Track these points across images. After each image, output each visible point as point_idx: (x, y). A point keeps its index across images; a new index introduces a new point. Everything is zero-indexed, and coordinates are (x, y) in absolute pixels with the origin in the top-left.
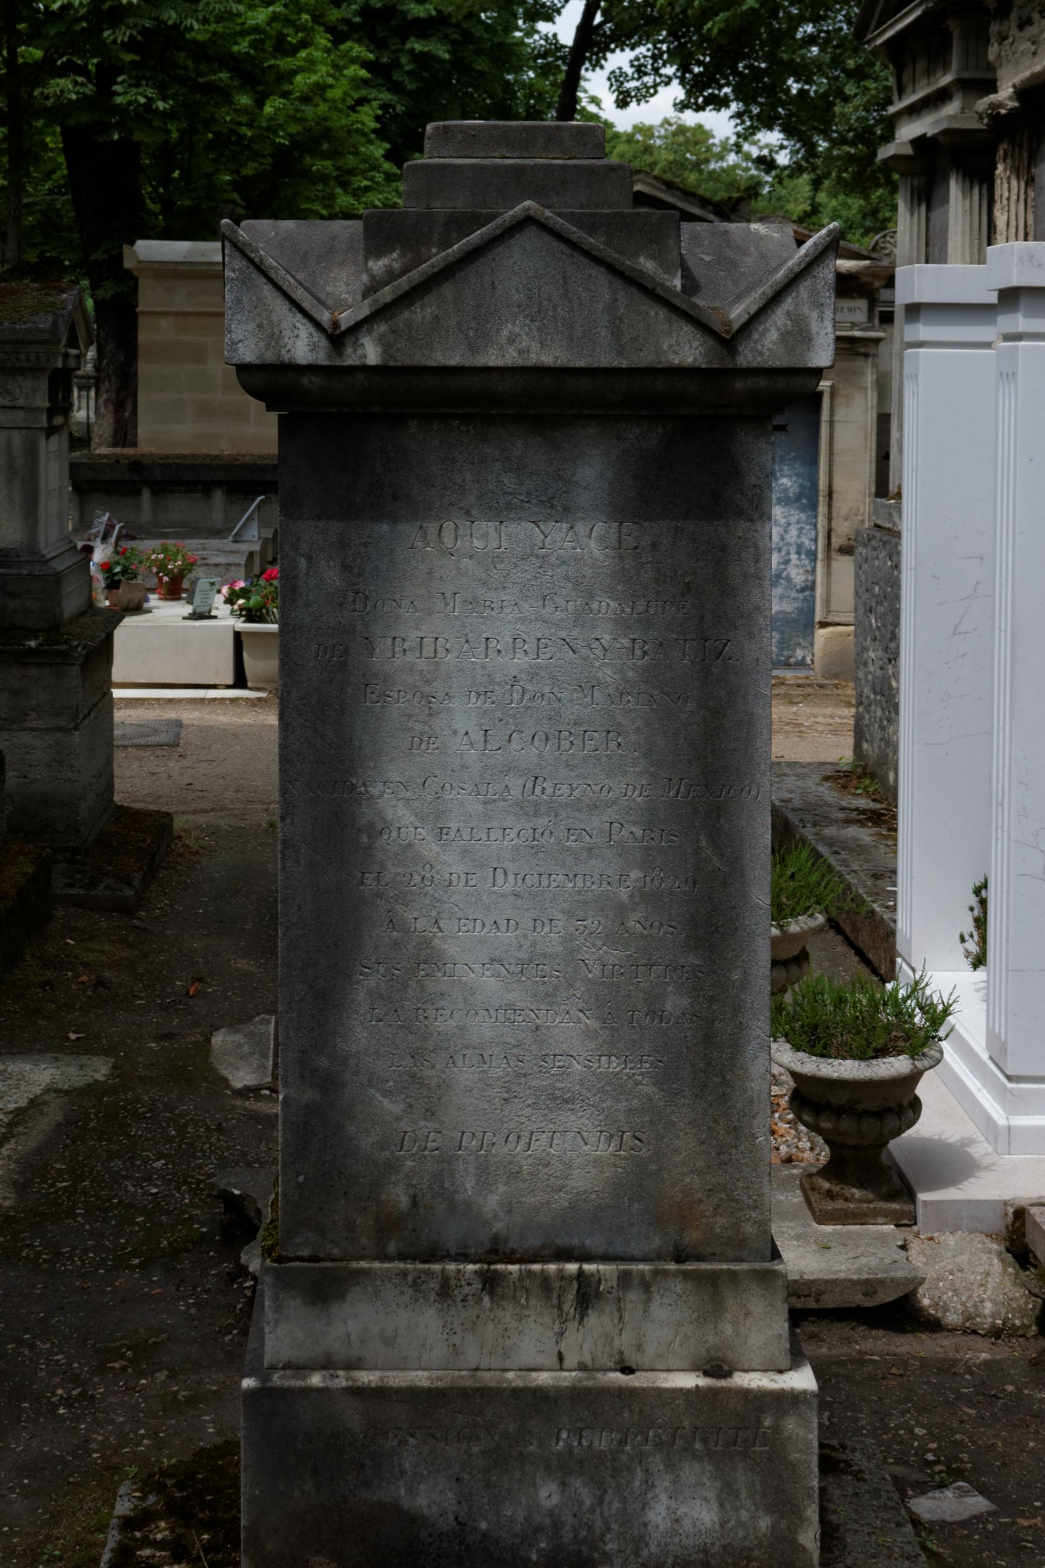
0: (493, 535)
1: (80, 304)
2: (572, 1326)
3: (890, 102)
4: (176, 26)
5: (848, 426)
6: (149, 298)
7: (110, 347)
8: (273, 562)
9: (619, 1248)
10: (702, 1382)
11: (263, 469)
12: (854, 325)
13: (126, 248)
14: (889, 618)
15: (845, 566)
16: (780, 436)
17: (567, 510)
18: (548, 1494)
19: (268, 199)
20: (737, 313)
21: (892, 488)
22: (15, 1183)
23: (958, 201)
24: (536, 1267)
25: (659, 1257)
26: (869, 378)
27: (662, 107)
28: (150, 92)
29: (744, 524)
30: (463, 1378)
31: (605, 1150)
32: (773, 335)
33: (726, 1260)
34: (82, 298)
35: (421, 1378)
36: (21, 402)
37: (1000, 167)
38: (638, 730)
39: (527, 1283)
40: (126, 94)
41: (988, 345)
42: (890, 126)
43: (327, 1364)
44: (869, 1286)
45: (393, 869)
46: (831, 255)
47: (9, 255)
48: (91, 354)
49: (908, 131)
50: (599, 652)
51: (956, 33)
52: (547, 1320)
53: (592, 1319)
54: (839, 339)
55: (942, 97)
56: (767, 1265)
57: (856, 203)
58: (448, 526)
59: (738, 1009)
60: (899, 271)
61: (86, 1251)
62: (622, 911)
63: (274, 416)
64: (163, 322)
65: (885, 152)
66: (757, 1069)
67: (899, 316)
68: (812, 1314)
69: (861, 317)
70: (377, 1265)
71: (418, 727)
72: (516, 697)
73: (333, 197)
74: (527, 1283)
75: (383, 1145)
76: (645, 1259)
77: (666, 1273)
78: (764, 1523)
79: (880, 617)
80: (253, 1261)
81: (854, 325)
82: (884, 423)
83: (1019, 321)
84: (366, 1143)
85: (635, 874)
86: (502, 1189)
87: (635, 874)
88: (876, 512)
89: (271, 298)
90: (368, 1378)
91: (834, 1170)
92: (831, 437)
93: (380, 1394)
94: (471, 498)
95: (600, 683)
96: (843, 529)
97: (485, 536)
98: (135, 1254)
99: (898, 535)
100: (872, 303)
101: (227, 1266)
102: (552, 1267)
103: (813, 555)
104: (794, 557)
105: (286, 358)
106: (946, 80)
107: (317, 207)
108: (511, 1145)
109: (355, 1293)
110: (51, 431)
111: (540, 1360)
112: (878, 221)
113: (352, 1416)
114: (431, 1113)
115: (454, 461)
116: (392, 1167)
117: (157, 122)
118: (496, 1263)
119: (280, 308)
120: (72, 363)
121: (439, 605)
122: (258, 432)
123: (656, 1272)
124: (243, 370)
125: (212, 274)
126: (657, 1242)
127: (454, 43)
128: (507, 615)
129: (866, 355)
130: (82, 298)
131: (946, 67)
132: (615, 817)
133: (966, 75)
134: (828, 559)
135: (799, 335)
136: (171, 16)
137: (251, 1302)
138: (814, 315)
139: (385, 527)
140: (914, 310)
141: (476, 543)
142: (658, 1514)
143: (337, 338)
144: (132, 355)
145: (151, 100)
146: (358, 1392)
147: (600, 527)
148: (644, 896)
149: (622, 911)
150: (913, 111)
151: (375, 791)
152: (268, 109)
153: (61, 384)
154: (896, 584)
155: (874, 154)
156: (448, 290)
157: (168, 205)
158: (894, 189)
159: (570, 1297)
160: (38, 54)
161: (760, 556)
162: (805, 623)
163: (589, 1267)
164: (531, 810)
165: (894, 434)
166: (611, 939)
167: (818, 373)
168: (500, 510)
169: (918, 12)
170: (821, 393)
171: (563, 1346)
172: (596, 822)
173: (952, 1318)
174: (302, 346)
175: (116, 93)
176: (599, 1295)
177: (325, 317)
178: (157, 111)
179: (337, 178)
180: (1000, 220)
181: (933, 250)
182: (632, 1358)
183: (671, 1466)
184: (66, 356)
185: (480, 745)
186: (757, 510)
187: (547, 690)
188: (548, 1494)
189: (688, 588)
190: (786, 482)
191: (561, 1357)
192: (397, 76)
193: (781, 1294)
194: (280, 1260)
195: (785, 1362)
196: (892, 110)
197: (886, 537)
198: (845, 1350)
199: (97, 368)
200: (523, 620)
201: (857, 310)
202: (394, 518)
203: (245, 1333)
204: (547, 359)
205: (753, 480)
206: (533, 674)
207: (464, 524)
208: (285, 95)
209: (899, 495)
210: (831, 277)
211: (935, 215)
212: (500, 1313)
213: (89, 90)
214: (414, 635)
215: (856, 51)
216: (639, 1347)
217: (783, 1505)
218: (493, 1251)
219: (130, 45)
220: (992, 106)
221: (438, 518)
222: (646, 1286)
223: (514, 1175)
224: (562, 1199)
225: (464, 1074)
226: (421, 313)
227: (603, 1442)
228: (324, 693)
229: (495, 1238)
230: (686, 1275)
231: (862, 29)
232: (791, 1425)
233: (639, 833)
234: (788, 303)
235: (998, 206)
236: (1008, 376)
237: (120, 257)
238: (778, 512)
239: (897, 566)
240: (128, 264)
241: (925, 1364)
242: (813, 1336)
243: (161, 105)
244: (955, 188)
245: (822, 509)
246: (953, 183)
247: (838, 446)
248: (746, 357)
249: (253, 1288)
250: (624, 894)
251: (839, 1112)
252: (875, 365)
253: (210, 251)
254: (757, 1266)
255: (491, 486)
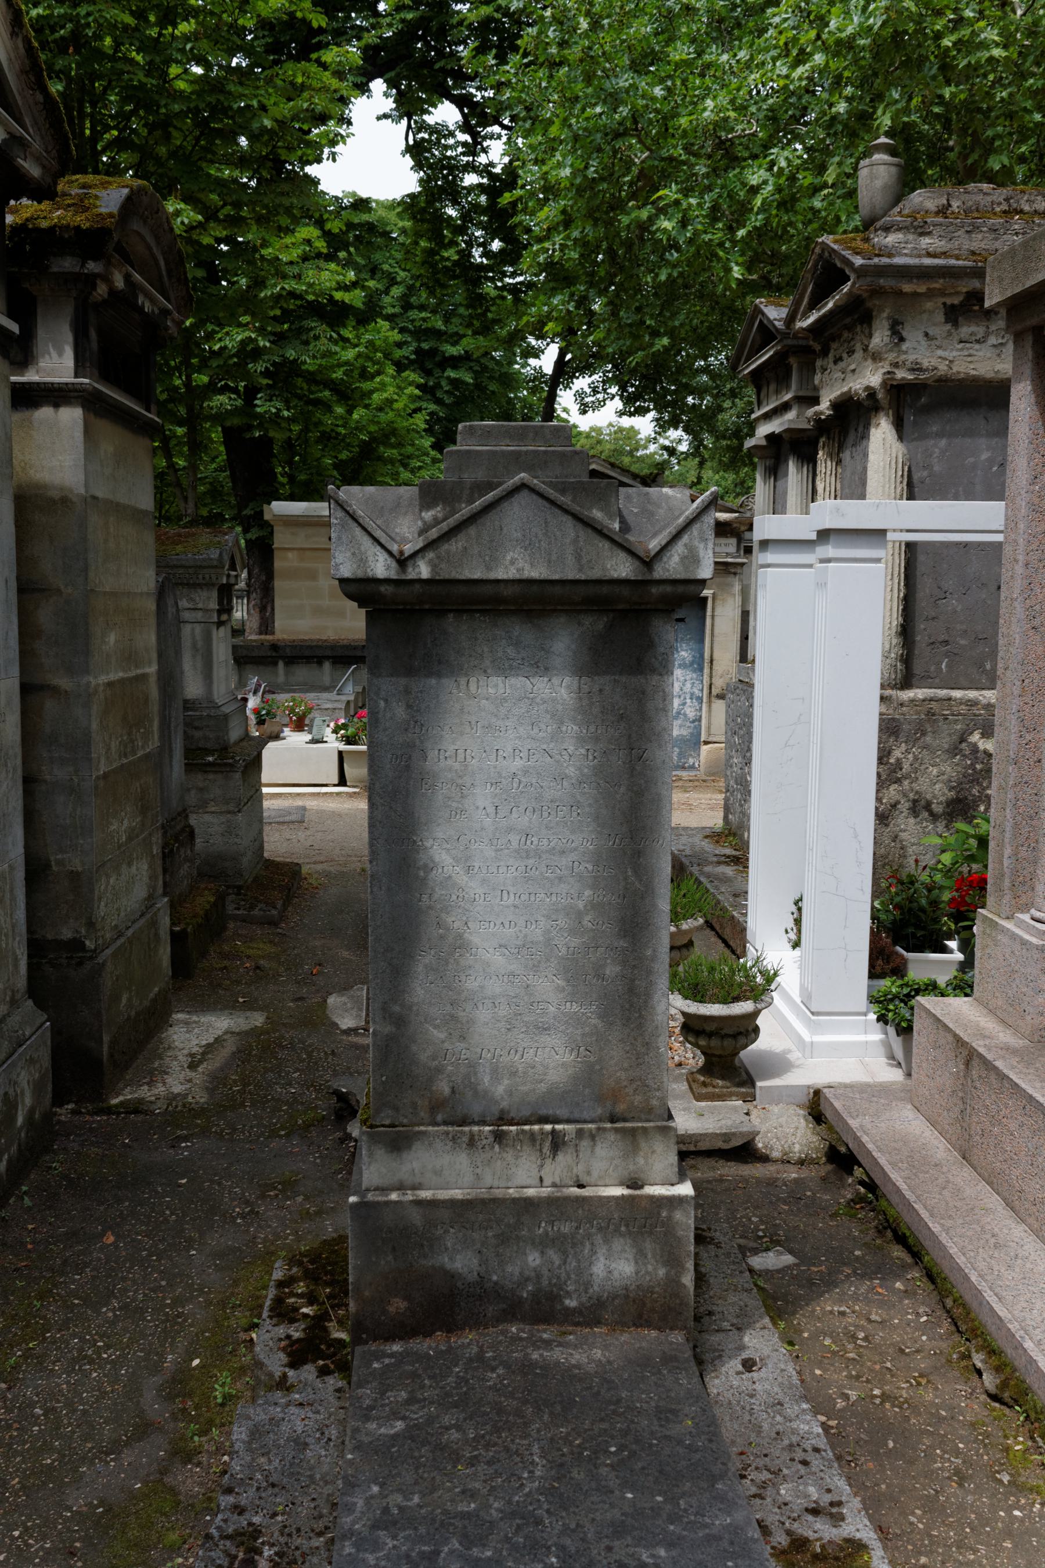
0: (501, 685)
1: (237, 542)
2: (548, 1161)
3: (752, 412)
4: (295, 360)
5: (723, 619)
6: (281, 539)
7: (256, 571)
8: (363, 706)
9: (576, 1115)
10: (626, 1192)
11: (355, 648)
12: (728, 554)
13: (265, 506)
14: (746, 738)
15: (719, 706)
16: (681, 625)
17: (547, 669)
18: (534, 1259)
19: (355, 473)
20: (654, 545)
21: (750, 657)
22: (207, 1088)
23: (794, 474)
24: (527, 1127)
25: (601, 1120)
26: (737, 588)
27: (608, 416)
28: (279, 405)
29: (656, 677)
30: (483, 1193)
31: (569, 1058)
32: (676, 559)
33: (641, 1120)
34: (236, 538)
35: (457, 1194)
36: (200, 606)
37: (821, 453)
38: (590, 805)
39: (521, 1137)
40: (262, 406)
41: (810, 566)
42: (752, 428)
43: (401, 1187)
44: (726, 1137)
45: (439, 892)
46: (713, 508)
47: (189, 511)
48: (244, 575)
49: (764, 430)
50: (567, 757)
51: (795, 366)
52: (533, 1158)
53: (560, 1157)
54: (716, 563)
55: (785, 407)
56: (665, 1123)
57: (731, 477)
58: (473, 680)
59: (649, 972)
60: (756, 520)
61: (252, 1127)
62: (580, 915)
63: (363, 611)
64: (290, 555)
65: (749, 443)
66: (661, 1008)
67: (756, 547)
68: (691, 1154)
69: (732, 549)
70: (430, 1128)
71: (454, 805)
72: (515, 785)
73: (398, 473)
74: (521, 1137)
75: (434, 1058)
76: (592, 1122)
77: (605, 1129)
78: (662, 1272)
79: (742, 737)
80: (355, 1129)
81: (728, 554)
82: (745, 616)
83: (829, 550)
84: (423, 1057)
85: (588, 893)
86: (506, 1082)
87: (588, 893)
88: (739, 672)
89: (358, 537)
90: (425, 1194)
91: (707, 1069)
92: (713, 625)
93: (433, 1203)
94: (487, 663)
95: (567, 776)
96: (719, 684)
97: (496, 686)
98: (282, 1128)
99: (752, 686)
100: (740, 540)
101: (339, 1134)
102: (536, 1127)
103: (700, 700)
104: (688, 701)
105: (370, 574)
106: (788, 397)
107: (388, 480)
108: (512, 1056)
109: (417, 1145)
110: (220, 624)
111: (529, 1182)
112: (745, 488)
113: (416, 1217)
114: (463, 1038)
115: (476, 639)
116: (439, 1070)
117: (283, 425)
119: (366, 542)
120: (232, 581)
121: (468, 730)
122: (351, 624)
123: (599, 1129)
124: (343, 581)
125: (323, 524)
126: (599, 1111)
127: (475, 372)
128: (509, 735)
129: (735, 574)
130: (236, 538)
131: (788, 388)
132: (575, 858)
133: (801, 394)
134: (710, 702)
135: (692, 559)
136: (291, 354)
137: (353, 1155)
138: (702, 546)
139: (433, 681)
140: (765, 544)
141: (490, 690)
142: (599, 1269)
143: (402, 561)
144: (269, 574)
145: (279, 410)
146: (419, 1203)
147: (567, 680)
148: (593, 906)
149: (580, 915)
150: (767, 417)
151: (428, 844)
152: (355, 416)
153: (226, 593)
154: (750, 716)
155: (742, 445)
156: (472, 531)
157: (292, 479)
158: (754, 469)
159: (547, 1144)
160: (205, 379)
161: (666, 697)
162: (695, 742)
163: (558, 1127)
164: (524, 855)
165: (751, 623)
166: (573, 932)
167: (703, 583)
168: (505, 669)
169: (771, 353)
170: (706, 599)
171: (542, 1173)
172: (564, 861)
173: (775, 1155)
174: (381, 567)
175: (256, 406)
176: (564, 1143)
177: (395, 548)
178: (283, 418)
179: (400, 461)
180: (820, 486)
181: (777, 506)
182: (584, 1179)
183: (606, 1241)
184: (228, 576)
185: (493, 815)
186: (665, 668)
187: (534, 781)
188: (534, 1259)
189: (622, 717)
190: (684, 654)
191: (541, 1179)
192: (439, 394)
193: (673, 1140)
194: (371, 1127)
195: (675, 1180)
196: (753, 416)
197: (745, 687)
198: (712, 1174)
199: (248, 585)
200: (520, 738)
201: (729, 545)
202: (439, 675)
203: (350, 1173)
204: (535, 574)
205: (662, 650)
206: (526, 772)
207: (483, 680)
208: (366, 406)
209: (753, 661)
210: (712, 521)
211: (779, 483)
212: (505, 1155)
213: (239, 402)
214: (451, 748)
215: (732, 379)
216: (589, 1173)
217: (673, 1261)
218: (501, 1119)
219: (266, 374)
220: (816, 413)
221: (466, 675)
222: (593, 1137)
223: (514, 1074)
224: (543, 1087)
225: (483, 1014)
226: (455, 546)
227: (566, 1228)
228: (396, 785)
229: (502, 1111)
230: (616, 1130)
231: (734, 364)
232: (678, 1215)
233: (590, 868)
234: (685, 539)
235: (818, 478)
236: (822, 585)
237: (261, 513)
238: (678, 673)
239: (752, 706)
240: (267, 517)
241: (759, 1181)
242: (692, 1167)
243: (286, 413)
244: (792, 466)
245: (706, 671)
246: (791, 463)
247: (716, 631)
248: (660, 572)
249: (355, 1147)
250: (581, 905)
251: (710, 1035)
252: (741, 580)
253: (320, 508)
254: (659, 1124)
255: (500, 654)
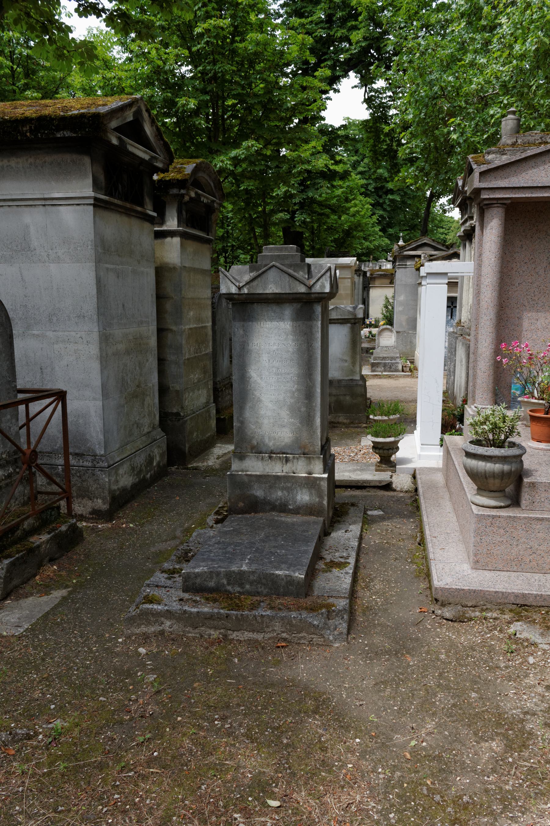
10: (306, 475)
18: (280, 493)
20: (312, 283)
30: (266, 474)
31: (291, 435)
32: (318, 286)
35: (258, 473)
43: (242, 471)
45: (253, 385)
53: (288, 464)
62: (294, 392)
78: (317, 500)
84: (249, 433)
109: (247, 459)
114: (260, 428)
116: (253, 437)
118: (272, 454)
119: (229, 283)
135: (323, 286)
142: (299, 497)
143: (240, 288)
148: (298, 390)
149: (294, 392)
156: (259, 279)
166: (291, 398)
168: (271, 320)
172: (289, 377)
174: (234, 290)
177: (237, 284)
182: (295, 471)
183: (301, 489)
188: (280, 493)
202: (252, 321)
204: (277, 291)
217: (321, 497)
222: (298, 459)
224: (283, 444)
225: (266, 421)
226: (255, 283)
227: (289, 485)
232: (322, 483)
234: (321, 280)
248: (313, 290)
250: (294, 389)
